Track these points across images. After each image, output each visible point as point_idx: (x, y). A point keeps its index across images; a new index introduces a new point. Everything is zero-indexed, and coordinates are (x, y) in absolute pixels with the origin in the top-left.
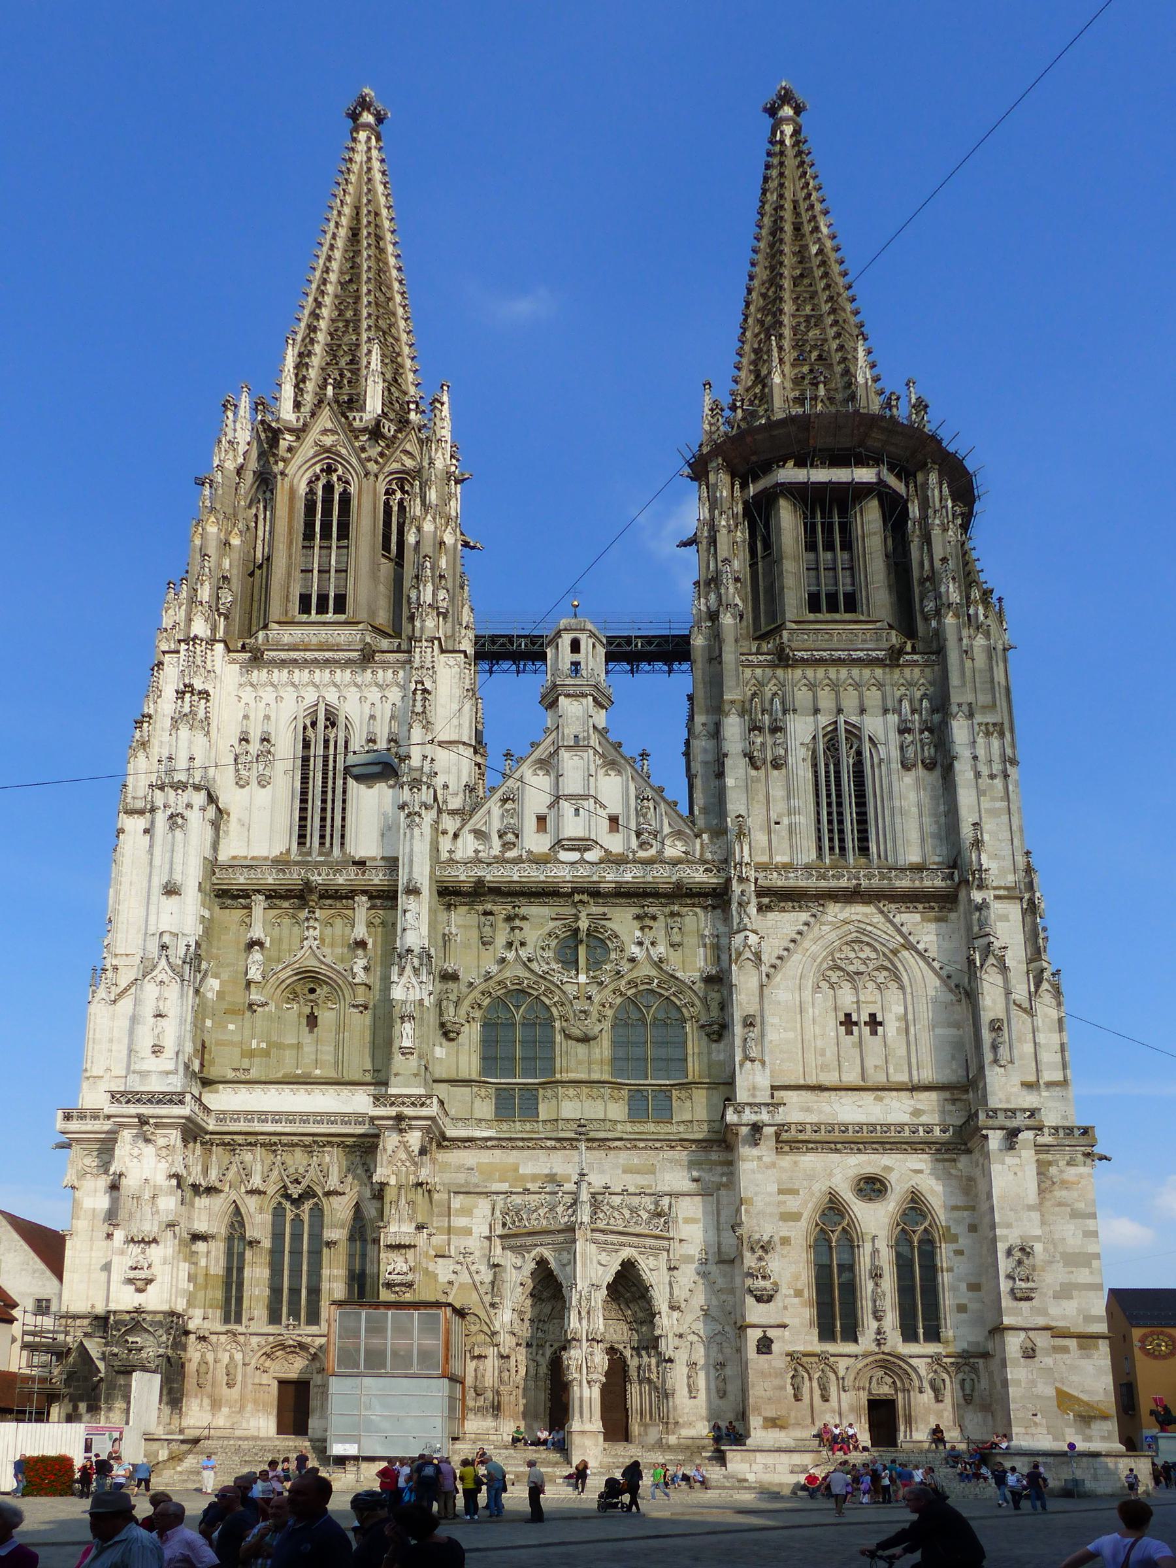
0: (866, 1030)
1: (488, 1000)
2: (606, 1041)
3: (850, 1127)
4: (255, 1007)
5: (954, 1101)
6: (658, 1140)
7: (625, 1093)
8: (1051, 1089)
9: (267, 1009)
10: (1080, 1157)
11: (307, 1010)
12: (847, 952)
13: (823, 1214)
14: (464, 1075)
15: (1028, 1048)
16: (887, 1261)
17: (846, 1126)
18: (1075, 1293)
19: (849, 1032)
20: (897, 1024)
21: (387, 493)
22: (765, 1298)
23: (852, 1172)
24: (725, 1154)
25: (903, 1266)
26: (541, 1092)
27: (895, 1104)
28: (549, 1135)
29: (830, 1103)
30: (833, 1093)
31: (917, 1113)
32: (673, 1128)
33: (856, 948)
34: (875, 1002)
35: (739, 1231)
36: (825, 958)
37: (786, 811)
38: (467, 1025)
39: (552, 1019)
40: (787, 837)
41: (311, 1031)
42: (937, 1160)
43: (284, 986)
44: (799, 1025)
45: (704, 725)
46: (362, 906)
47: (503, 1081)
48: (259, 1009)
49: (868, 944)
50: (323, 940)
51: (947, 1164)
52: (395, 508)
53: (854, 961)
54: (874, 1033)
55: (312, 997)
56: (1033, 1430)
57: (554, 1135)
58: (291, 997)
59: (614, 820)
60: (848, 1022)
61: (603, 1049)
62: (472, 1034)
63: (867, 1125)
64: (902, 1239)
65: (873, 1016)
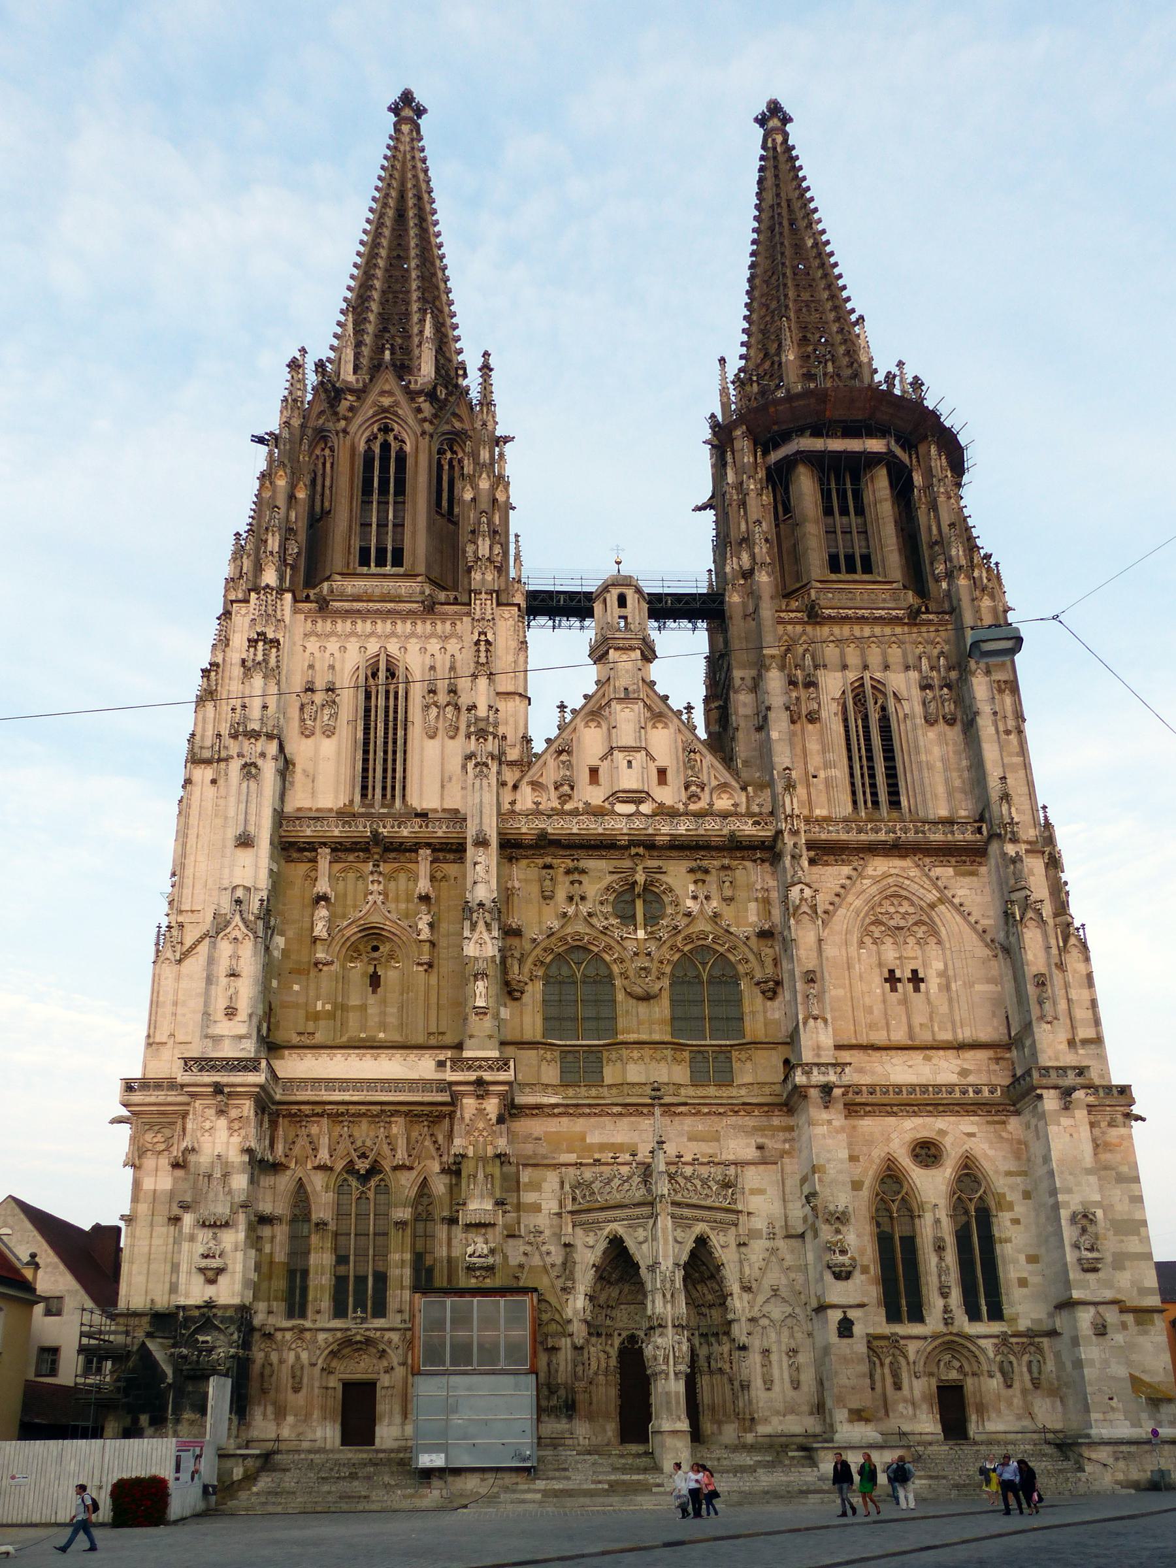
1: (551, 957)
2: (665, 1001)
3: (904, 1089)
4: (320, 966)
5: (997, 1060)
6: (721, 1104)
7: (686, 1054)
8: (1087, 1047)
9: (333, 968)
10: (1120, 1118)
11: (371, 969)
13: (882, 1182)
14: (528, 1036)
15: (1062, 1005)
16: (947, 1231)
17: (899, 1086)
18: (1127, 1264)
19: (894, 989)
20: (938, 980)
21: (439, 452)
22: (843, 1274)
23: (909, 1137)
24: (786, 1118)
25: (963, 1238)
26: (605, 1054)
27: (944, 1064)
28: (615, 1100)
29: (882, 1063)
31: (964, 1073)
32: (733, 1092)
33: (896, 902)
34: (916, 958)
35: (814, 1202)
36: (867, 915)
38: (530, 983)
39: (611, 976)
40: (824, 790)
41: (374, 992)
42: (988, 1122)
43: (349, 944)
45: (742, 679)
46: (424, 863)
47: (568, 1043)
48: (325, 968)
49: (906, 898)
52: (446, 467)
54: (917, 989)
55: (376, 954)
56: (1111, 1416)
57: (620, 1100)
58: (355, 955)
59: (662, 772)
61: (662, 1009)
62: (534, 992)
63: (919, 1085)
64: (958, 1206)
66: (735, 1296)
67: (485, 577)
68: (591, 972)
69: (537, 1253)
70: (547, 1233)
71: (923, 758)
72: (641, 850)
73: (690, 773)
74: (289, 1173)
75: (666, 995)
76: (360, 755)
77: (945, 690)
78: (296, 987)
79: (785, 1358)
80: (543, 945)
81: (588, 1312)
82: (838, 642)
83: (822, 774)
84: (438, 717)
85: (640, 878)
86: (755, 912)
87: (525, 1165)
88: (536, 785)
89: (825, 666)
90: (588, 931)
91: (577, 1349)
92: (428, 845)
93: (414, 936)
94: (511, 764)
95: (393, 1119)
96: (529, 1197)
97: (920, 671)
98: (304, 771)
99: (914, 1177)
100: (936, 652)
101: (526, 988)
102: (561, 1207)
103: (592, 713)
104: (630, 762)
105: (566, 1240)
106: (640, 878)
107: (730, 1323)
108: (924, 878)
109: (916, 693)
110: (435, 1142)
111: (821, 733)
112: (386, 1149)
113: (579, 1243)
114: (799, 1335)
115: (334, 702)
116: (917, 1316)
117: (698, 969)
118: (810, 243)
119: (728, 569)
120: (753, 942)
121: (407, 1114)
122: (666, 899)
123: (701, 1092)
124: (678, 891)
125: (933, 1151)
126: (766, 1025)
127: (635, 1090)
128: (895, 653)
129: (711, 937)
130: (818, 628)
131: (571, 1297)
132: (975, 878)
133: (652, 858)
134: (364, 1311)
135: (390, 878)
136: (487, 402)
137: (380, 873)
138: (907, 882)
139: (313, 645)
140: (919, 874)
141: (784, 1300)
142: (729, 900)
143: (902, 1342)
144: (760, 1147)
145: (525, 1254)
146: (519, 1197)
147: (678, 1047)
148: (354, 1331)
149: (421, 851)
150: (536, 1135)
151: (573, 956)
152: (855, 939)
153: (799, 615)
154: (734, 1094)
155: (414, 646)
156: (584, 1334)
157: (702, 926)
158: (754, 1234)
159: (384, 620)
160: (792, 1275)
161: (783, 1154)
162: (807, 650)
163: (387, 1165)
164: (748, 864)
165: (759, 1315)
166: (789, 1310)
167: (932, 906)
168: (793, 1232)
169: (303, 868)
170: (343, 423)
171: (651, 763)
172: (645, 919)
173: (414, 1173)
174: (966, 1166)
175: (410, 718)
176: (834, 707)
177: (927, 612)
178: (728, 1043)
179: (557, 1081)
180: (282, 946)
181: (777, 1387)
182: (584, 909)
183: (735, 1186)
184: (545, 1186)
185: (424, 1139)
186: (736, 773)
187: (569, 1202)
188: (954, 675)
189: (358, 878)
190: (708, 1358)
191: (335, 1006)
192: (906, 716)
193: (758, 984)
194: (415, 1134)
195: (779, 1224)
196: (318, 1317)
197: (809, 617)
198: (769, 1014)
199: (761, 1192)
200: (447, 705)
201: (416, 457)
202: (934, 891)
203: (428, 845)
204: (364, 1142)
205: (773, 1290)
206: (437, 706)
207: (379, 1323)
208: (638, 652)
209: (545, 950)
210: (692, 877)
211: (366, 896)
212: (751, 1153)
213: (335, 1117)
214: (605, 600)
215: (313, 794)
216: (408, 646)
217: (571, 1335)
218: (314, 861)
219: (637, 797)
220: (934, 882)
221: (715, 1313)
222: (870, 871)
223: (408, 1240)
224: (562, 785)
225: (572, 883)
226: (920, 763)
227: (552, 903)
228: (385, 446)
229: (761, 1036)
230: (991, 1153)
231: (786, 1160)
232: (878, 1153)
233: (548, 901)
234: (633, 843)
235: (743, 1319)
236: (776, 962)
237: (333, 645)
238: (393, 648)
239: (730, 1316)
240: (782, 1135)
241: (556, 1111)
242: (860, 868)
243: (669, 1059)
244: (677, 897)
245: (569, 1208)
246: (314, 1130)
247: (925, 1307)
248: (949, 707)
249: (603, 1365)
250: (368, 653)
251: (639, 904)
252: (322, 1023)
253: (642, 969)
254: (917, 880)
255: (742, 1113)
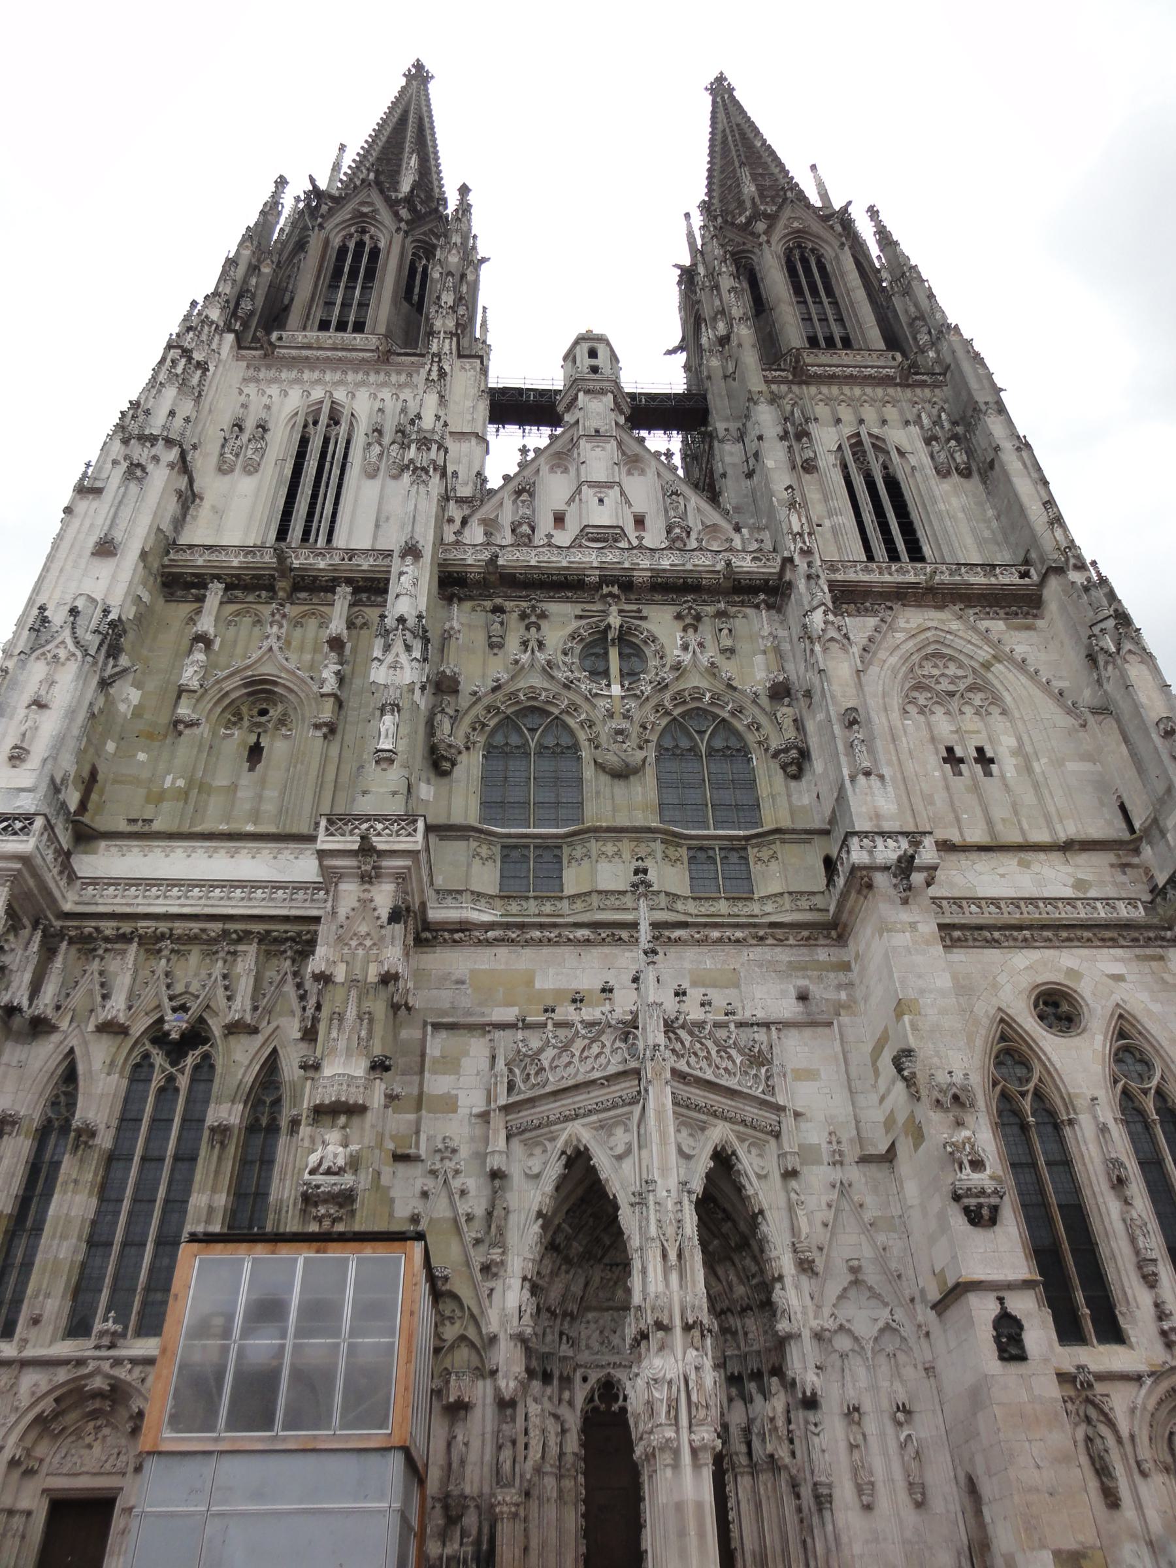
0: (978, 768)
4: (181, 727)
7: (683, 852)
9: (196, 731)
12: (928, 669)
23: (1026, 981)
26: (566, 851)
30: (962, 856)
31: (1079, 884)
32: (756, 908)
37: (825, 514)
39: (575, 747)
43: (227, 701)
44: (894, 758)
45: (727, 430)
47: (513, 831)
48: (187, 732)
50: (288, 643)
51: (1154, 964)
53: (941, 680)
60: (951, 758)
65: (980, 750)
66: (788, 1281)
67: (443, 323)
68: (550, 741)
69: (444, 1194)
70: (464, 1152)
71: (942, 506)
72: (615, 590)
73: (672, 513)
74: (55, 1038)
75: (650, 771)
76: (284, 491)
77: (953, 443)
78: (142, 756)
79: (890, 1429)
80: (486, 701)
81: (527, 1318)
82: (827, 401)
83: (827, 523)
84: (381, 455)
85: (615, 620)
86: (763, 667)
87: (437, 1026)
88: (490, 526)
89: (816, 419)
90: (546, 685)
91: (505, 1405)
92: (349, 581)
93: (315, 688)
94: (461, 501)
95: (240, 948)
96: (437, 1084)
97: (922, 427)
98: (213, 507)
99: (1048, 1049)
100: (935, 411)
101: (459, 758)
102: (489, 1102)
103: (558, 454)
104: (601, 501)
105: (495, 1162)
106: (615, 620)
107: (781, 1343)
108: (970, 632)
109: (920, 445)
110: (299, 986)
111: (821, 483)
112: (221, 993)
113: (516, 1172)
114: (909, 1372)
115: (263, 438)
116: (1112, 1332)
117: (692, 739)
118: (759, 144)
119: (704, 340)
120: (764, 701)
121: (263, 938)
122: (649, 651)
123: (707, 908)
124: (663, 639)
125: (1065, 1007)
126: (792, 813)
127: (612, 901)
128: (891, 412)
129: (708, 695)
130: (804, 387)
131: (498, 1284)
132: (1032, 633)
133: (628, 602)
134: (123, 1319)
135: (297, 623)
136: (465, 209)
137: (284, 616)
138: (948, 636)
139: (251, 389)
140: (962, 627)
141: (875, 1295)
142: (729, 652)
143: (1099, 1388)
144: (803, 997)
145: (425, 1195)
146: (421, 1084)
147: (672, 839)
148: (92, 1365)
149: (338, 589)
150: (457, 975)
151: (526, 721)
152: (895, 702)
153: (783, 374)
154: (757, 911)
155: (363, 395)
156: (519, 1368)
157: (695, 681)
158: (808, 1154)
159: (334, 370)
160: (881, 1238)
161: (839, 1008)
162: (793, 405)
163: (216, 1026)
164: (750, 611)
165: (830, 1324)
166: (884, 1314)
167: (987, 666)
168: (871, 1150)
169: (185, 609)
170: (320, 220)
171: (626, 507)
172: (622, 676)
173: (259, 1039)
174: (1122, 1035)
175: (350, 459)
176: (832, 459)
177: (917, 374)
178: (741, 833)
179: (493, 890)
180: (135, 702)
181: (883, 1503)
182: (541, 657)
183: (770, 1062)
184: (466, 1063)
185: (283, 981)
186: (726, 513)
187: (502, 1089)
188: (959, 430)
189: (255, 623)
190: (747, 1431)
191: (190, 782)
192: (913, 468)
193: (775, 755)
194: (270, 974)
195: (847, 1134)
196: (33, 1333)
197: (794, 376)
198: (794, 798)
199: (810, 1075)
200: (393, 443)
201: (388, 252)
202: (986, 647)
203: (349, 581)
204: (187, 986)
205: (854, 1270)
206: (380, 445)
207: (146, 1347)
208: (610, 396)
209: (488, 709)
210: (679, 625)
211: (262, 641)
212: (787, 1008)
213: (151, 944)
214: (575, 357)
215: (219, 530)
216: (357, 394)
217: (493, 1373)
218: (201, 599)
219: (607, 537)
220: (985, 635)
221: (752, 1324)
222: (901, 623)
223: (228, 1167)
224: (520, 524)
225: (528, 628)
226: (939, 514)
227: (501, 653)
228: (360, 245)
229: (786, 823)
230: (1156, 1008)
231: (845, 1019)
232: (985, 1009)
233: (496, 651)
234: (605, 580)
235: (806, 1334)
236: (799, 724)
237: (274, 390)
238: (340, 395)
239: (782, 1326)
240: (833, 977)
241: (490, 934)
242: (889, 619)
243: (659, 855)
244: (663, 647)
245: (503, 1100)
246: (113, 965)
247: (1120, 1309)
248: (960, 457)
249: (554, 1450)
250: (312, 398)
251: (613, 654)
252: (166, 806)
253: (620, 732)
254: (960, 633)
255: (770, 941)
